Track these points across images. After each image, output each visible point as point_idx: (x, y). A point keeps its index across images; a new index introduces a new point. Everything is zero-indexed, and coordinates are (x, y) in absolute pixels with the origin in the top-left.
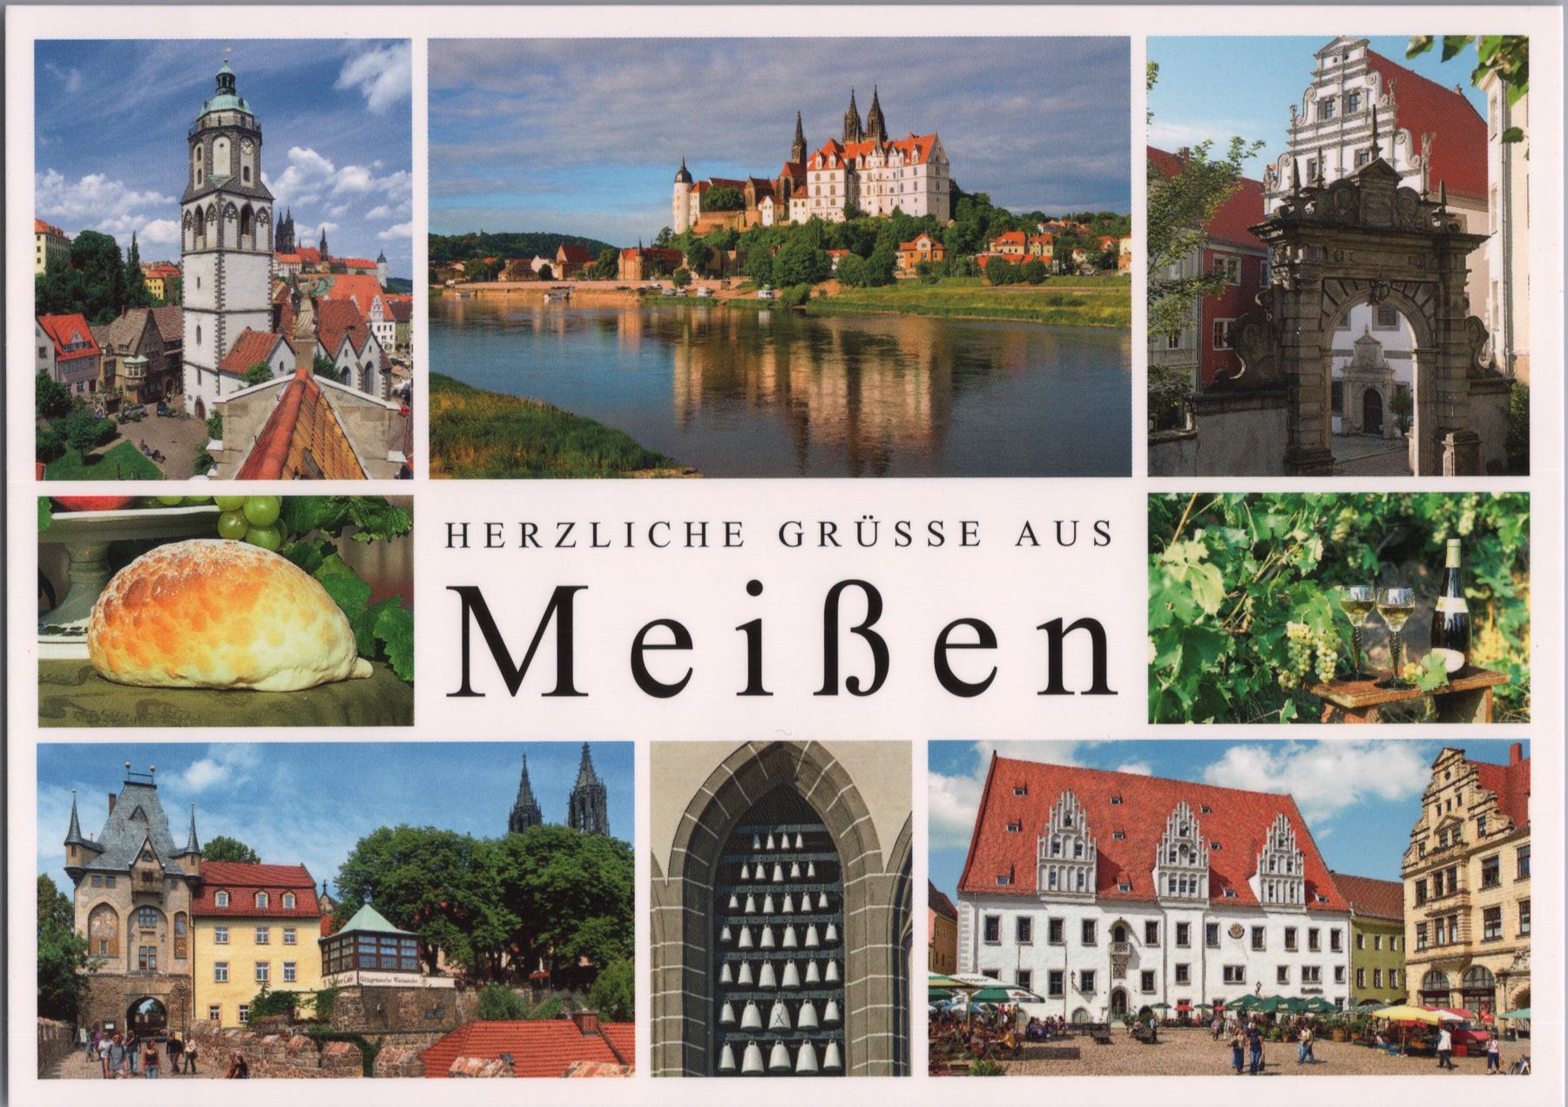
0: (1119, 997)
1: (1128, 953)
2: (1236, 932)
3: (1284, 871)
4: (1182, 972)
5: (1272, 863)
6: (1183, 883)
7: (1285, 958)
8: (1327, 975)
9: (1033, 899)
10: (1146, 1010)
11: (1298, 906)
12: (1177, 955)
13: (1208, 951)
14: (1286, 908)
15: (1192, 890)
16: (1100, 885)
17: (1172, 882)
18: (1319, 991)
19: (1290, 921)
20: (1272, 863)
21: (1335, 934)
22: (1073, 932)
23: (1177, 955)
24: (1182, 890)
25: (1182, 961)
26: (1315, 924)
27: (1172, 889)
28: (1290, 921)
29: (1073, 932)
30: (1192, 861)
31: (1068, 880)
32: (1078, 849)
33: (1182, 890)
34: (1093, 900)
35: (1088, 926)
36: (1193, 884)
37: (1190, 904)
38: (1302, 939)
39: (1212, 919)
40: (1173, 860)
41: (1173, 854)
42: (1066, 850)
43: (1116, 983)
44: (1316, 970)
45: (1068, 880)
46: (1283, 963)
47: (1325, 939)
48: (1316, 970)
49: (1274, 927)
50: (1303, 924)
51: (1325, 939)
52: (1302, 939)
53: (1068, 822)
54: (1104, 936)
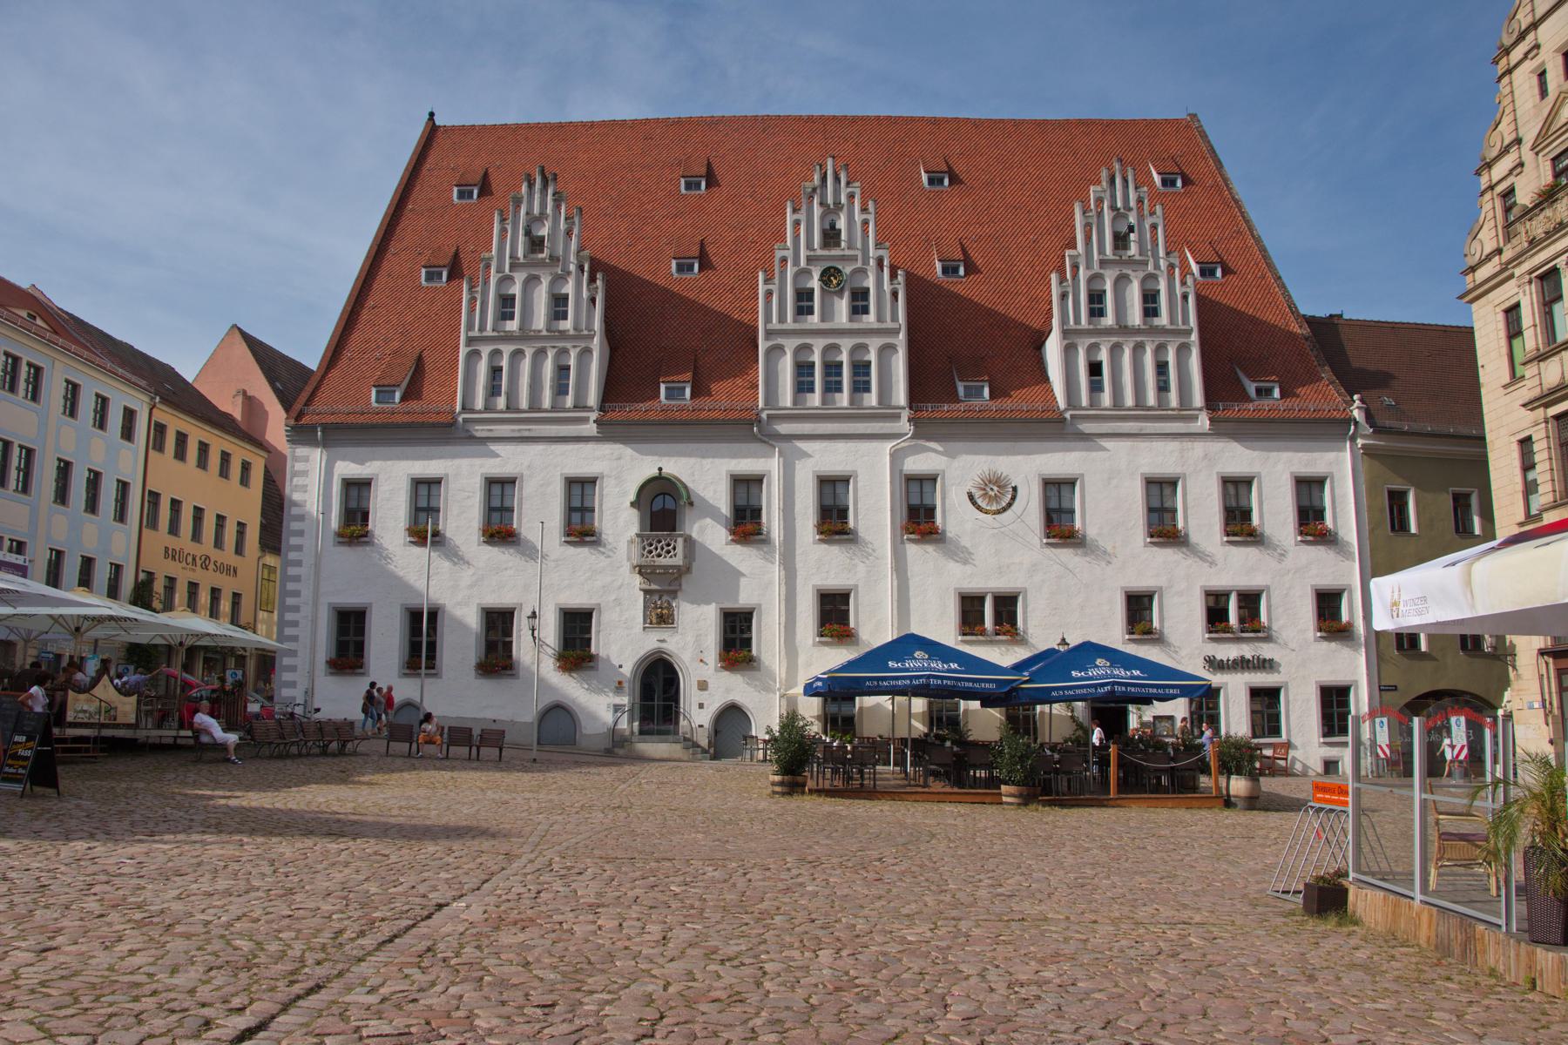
0: (658, 685)
1: (678, 560)
2: (995, 496)
3: (1135, 317)
4: (834, 612)
5: (1096, 298)
6: (832, 369)
7: (1151, 567)
8: (1292, 615)
9: (445, 431)
10: (732, 716)
11: (1185, 412)
12: (824, 566)
13: (914, 551)
14: (1145, 418)
15: (861, 387)
16: (612, 391)
17: (803, 370)
18: (1265, 665)
19: (1161, 457)
20: (1096, 298)
21: (1309, 489)
22: (541, 513)
23: (824, 566)
24: (832, 387)
25: (834, 582)
26: (1237, 457)
27: (803, 386)
28: (1161, 457)
29: (541, 513)
30: (859, 309)
31: (530, 377)
32: (558, 304)
33: (832, 387)
34: (591, 429)
35: (580, 490)
36: (861, 369)
37: (860, 424)
38: (1200, 511)
39: (918, 464)
40: (803, 310)
41: (804, 296)
42: (535, 311)
43: (651, 642)
44: (1250, 601)
45: (530, 377)
46: (1141, 583)
47: (1274, 509)
48: (1250, 601)
49: (1110, 479)
50: (1203, 464)
51: (1274, 509)
52: (1200, 511)
53: (536, 244)
54: (619, 519)
